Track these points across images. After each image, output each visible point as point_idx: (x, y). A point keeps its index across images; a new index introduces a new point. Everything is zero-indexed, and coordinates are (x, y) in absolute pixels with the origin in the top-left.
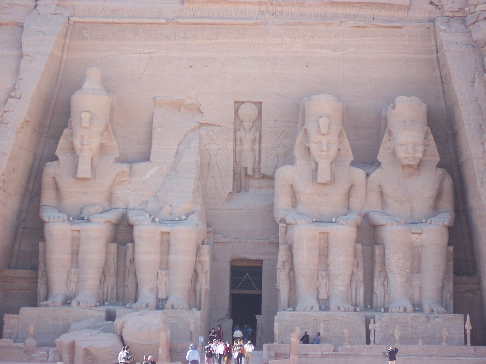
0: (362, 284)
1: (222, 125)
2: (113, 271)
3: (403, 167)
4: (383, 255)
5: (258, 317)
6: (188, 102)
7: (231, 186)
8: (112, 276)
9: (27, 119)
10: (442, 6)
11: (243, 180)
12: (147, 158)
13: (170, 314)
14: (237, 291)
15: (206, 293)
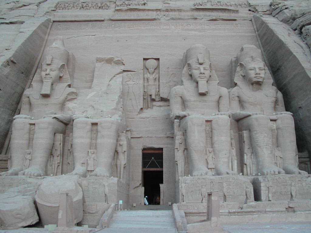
0: (236, 158)
1: (136, 71)
2: (58, 153)
3: (252, 84)
4: (251, 138)
5: (161, 185)
6: (117, 59)
7: (142, 104)
8: (58, 156)
9: (12, 59)
10: (257, 10)
11: (149, 103)
12: (90, 88)
13: (93, 181)
14: (146, 169)
15: (124, 167)
